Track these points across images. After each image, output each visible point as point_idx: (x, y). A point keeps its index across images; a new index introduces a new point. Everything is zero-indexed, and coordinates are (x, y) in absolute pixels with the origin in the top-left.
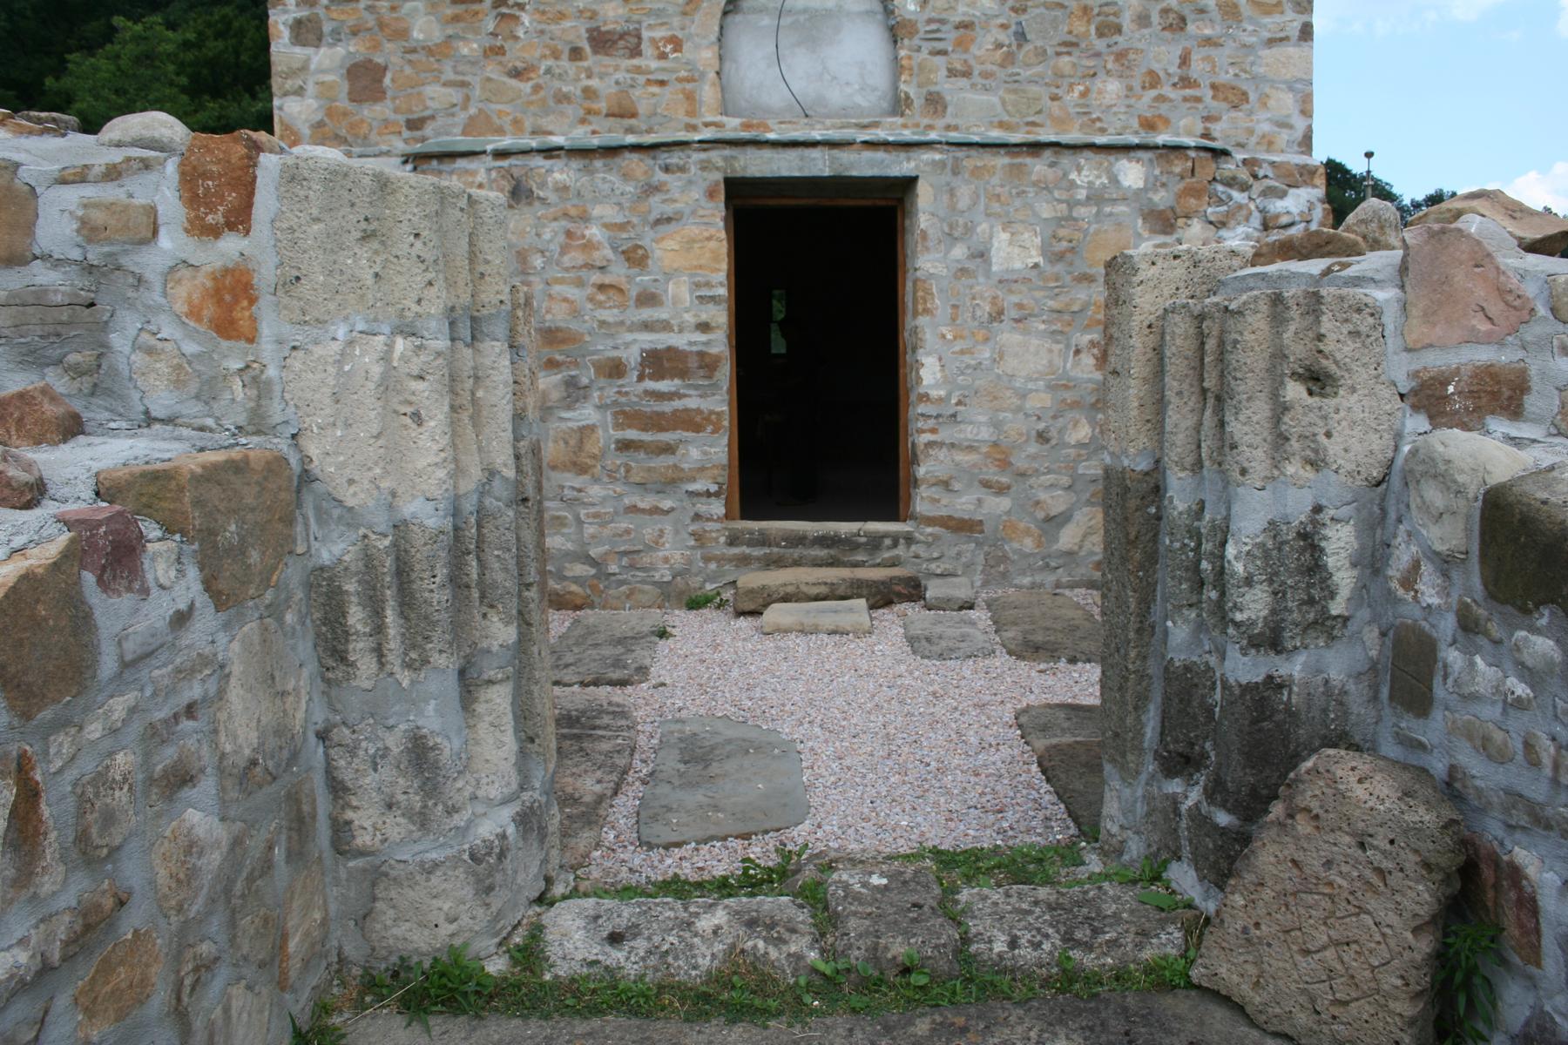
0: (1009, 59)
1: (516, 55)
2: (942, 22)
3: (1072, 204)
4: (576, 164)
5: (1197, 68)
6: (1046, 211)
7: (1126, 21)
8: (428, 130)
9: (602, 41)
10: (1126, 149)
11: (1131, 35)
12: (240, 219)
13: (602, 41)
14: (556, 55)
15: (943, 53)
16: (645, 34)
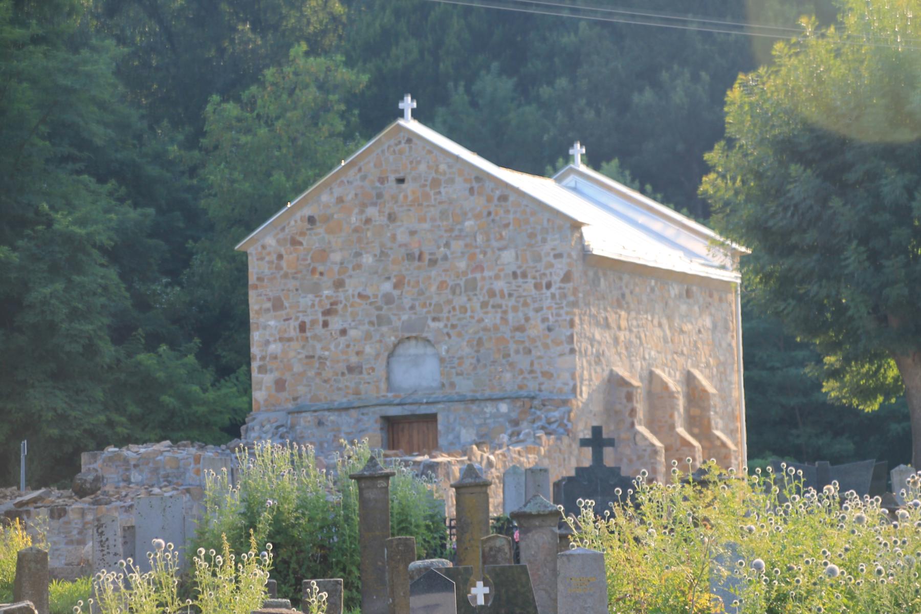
0: (475, 368)
1: (325, 375)
2: (454, 357)
3: (485, 419)
4: (336, 413)
5: (536, 367)
6: (477, 422)
7: (512, 353)
8: (299, 401)
9: (351, 369)
10: (502, 399)
11: (514, 357)
12: (199, 463)
13: (351, 369)
14: (337, 375)
15: (454, 368)
16: (364, 367)
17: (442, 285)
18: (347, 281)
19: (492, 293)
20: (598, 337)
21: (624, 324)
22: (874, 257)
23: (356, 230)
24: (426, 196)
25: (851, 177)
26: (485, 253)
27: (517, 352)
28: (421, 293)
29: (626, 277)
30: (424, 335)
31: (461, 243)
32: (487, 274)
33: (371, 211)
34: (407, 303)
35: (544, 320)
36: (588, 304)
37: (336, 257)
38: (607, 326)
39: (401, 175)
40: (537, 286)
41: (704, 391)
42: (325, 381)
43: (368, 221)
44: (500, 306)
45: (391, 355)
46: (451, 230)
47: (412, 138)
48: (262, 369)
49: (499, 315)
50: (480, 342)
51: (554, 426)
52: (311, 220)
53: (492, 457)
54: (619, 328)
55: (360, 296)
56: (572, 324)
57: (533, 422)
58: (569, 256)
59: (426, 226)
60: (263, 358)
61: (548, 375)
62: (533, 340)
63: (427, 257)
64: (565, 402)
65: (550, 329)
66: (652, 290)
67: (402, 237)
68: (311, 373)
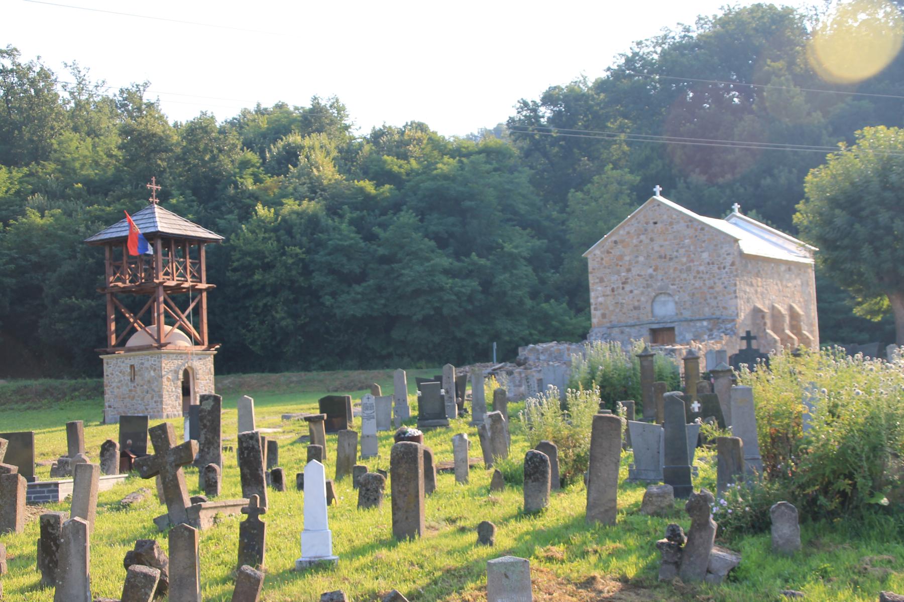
6: (693, 330)
9: (635, 308)
10: (704, 320)
11: (709, 301)
17: (675, 269)
18: (633, 269)
19: (698, 272)
20: (748, 290)
21: (760, 284)
22: (876, 250)
23: (636, 246)
24: (667, 229)
25: (864, 213)
26: (694, 254)
27: (711, 298)
28: (666, 273)
29: (760, 263)
30: (668, 292)
31: (683, 250)
32: (695, 263)
33: (643, 237)
34: (660, 277)
35: (723, 283)
36: (743, 276)
37: (627, 258)
38: (752, 285)
39: (655, 221)
40: (719, 268)
41: (798, 313)
42: (624, 314)
43: (641, 242)
44: (702, 278)
45: (653, 301)
46: (679, 244)
47: (660, 204)
48: (596, 309)
49: (702, 282)
50: (693, 294)
51: (729, 331)
52: (616, 242)
53: (700, 346)
54: (758, 286)
55: (639, 275)
56: (735, 285)
57: (719, 329)
58: (734, 254)
59: (667, 243)
60: (596, 304)
61: (725, 308)
62: (718, 293)
63: (668, 257)
64: (733, 320)
65: (725, 287)
66: (773, 268)
67: (657, 248)
68: (617, 310)
